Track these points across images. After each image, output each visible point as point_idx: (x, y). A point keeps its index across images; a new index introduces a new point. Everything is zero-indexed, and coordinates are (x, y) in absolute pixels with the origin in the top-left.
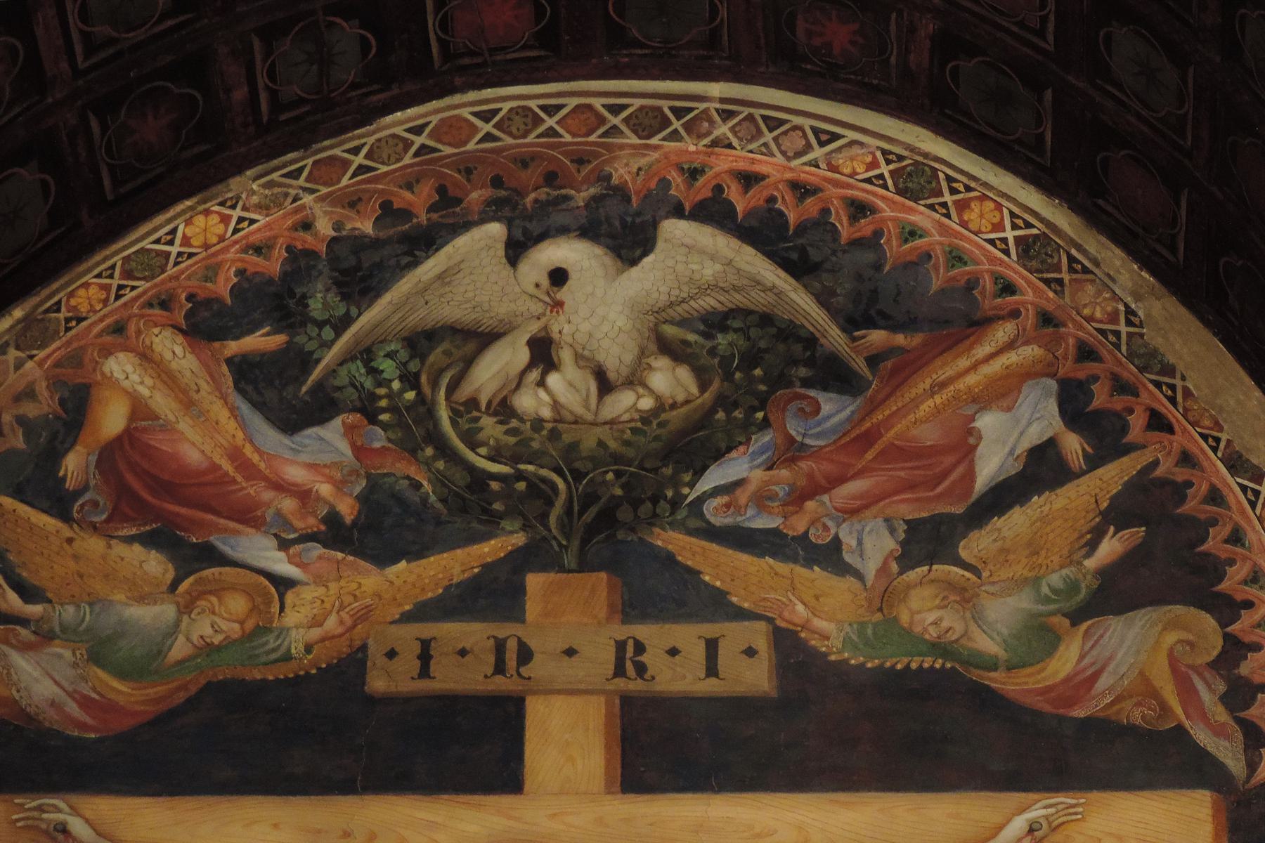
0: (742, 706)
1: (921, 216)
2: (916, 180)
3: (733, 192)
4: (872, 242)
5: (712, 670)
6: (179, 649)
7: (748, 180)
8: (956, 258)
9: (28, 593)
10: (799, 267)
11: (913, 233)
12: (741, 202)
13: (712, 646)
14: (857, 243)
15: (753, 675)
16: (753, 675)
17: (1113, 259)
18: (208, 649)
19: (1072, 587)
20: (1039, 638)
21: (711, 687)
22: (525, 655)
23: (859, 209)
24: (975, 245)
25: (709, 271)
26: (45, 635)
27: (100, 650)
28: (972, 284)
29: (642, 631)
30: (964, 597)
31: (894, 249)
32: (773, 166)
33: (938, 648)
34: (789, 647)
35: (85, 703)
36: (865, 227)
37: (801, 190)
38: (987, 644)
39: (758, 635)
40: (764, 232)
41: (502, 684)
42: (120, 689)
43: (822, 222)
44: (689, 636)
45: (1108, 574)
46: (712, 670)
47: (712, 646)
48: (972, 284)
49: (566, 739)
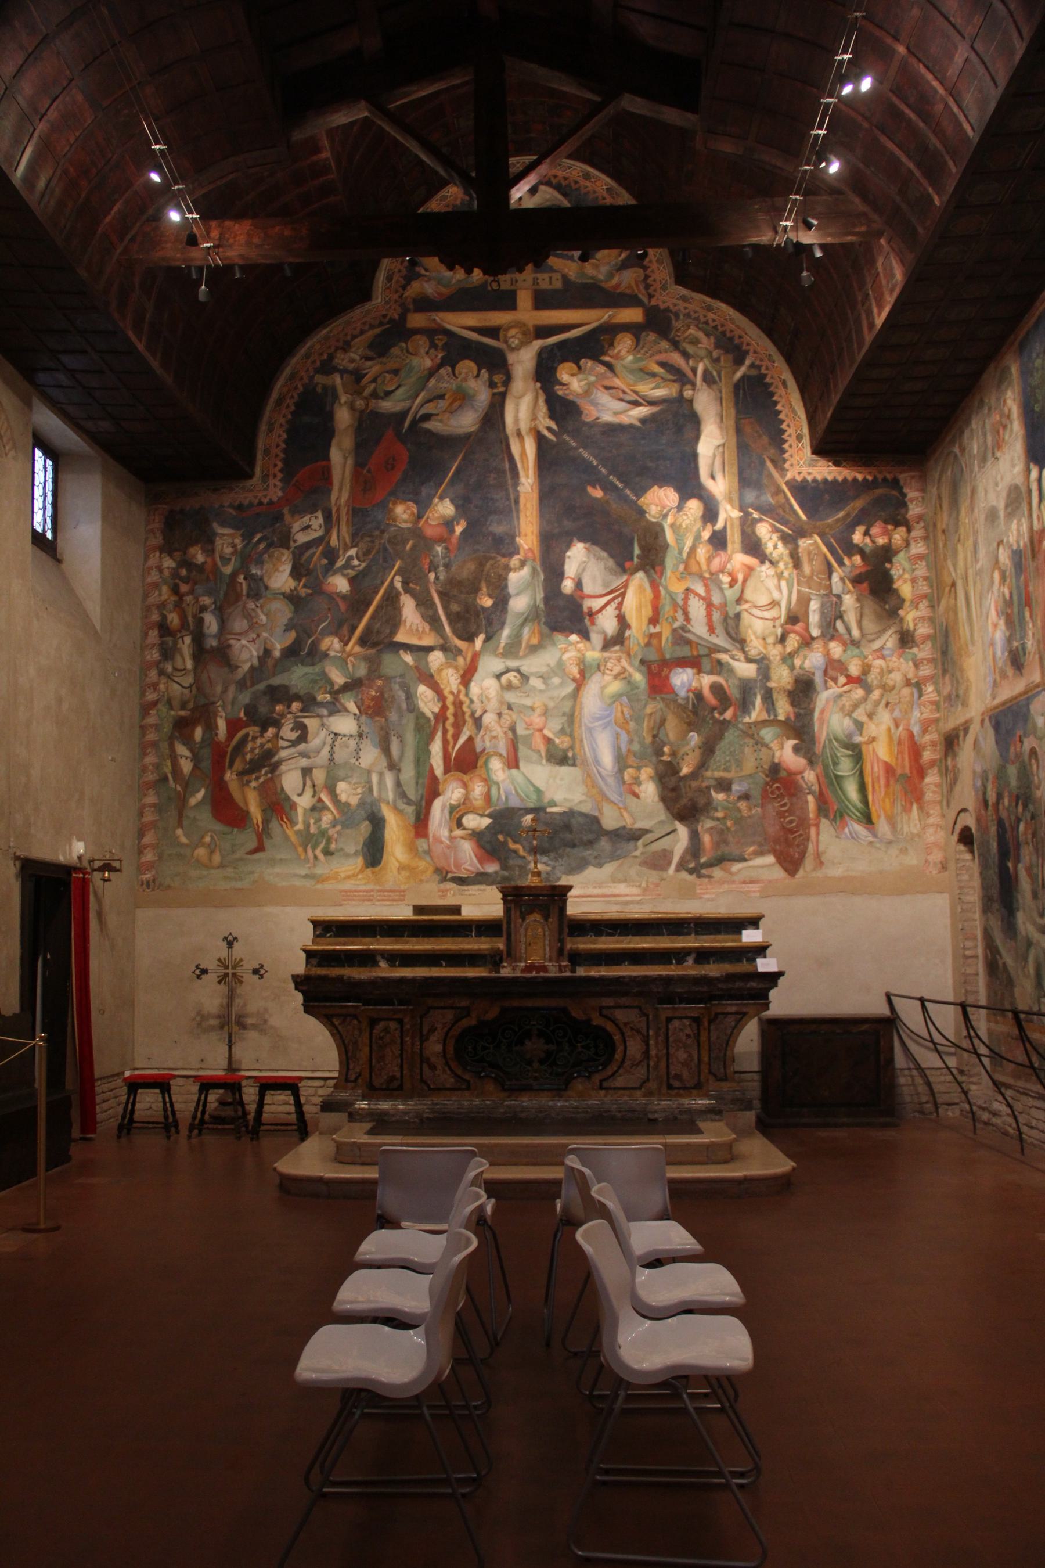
0: (556, 291)
1: (587, 183)
2: (587, 176)
3: (552, 179)
4: (578, 189)
5: (551, 283)
6: (454, 281)
7: (555, 176)
8: (595, 192)
9: (426, 270)
10: (565, 195)
11: (586, 187)
12: (554, 181)
13: (550, 278)
14: (576, 189)
15: (558, 285)
16: (558, 285)
17: (624, 192)
18: (459, 281)
19: (616, 264)
20: (610, 275)
21: (550, 287)
22: (517, 281)
23: (576, 182)
24: (598, 189)
25: (548, 196)
26: (430, 279)
27: (439, 282)
28: (597, 198)
29: (539, 275)
30: (596, 267)
31: (583, 191)
32: (560, 174)
33: (592, 278)
34: (565, 277)
35: (438, 293)
36: (577, 186)
37: (565, 179)
38: (601, 277)
39: (559, 276)
40: (558, 188)
41: (512, 288)
42: (444, 290)
43: (569, 185)
44: (546, 276)
45: (623, 261)
46: (551, 283)
47: (550, 278)
48: (597, 198)
49: (524, 299)
